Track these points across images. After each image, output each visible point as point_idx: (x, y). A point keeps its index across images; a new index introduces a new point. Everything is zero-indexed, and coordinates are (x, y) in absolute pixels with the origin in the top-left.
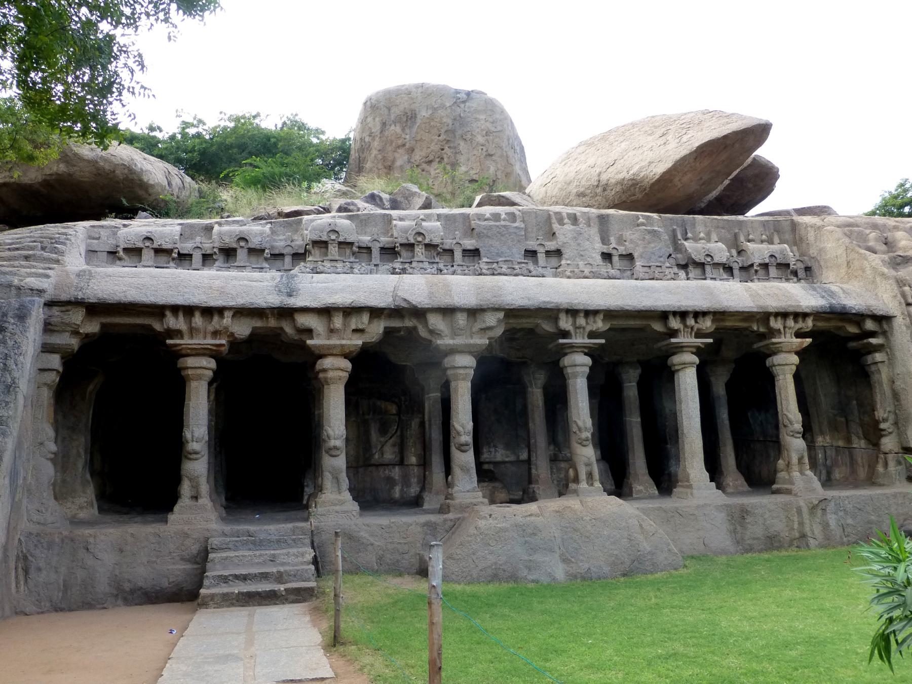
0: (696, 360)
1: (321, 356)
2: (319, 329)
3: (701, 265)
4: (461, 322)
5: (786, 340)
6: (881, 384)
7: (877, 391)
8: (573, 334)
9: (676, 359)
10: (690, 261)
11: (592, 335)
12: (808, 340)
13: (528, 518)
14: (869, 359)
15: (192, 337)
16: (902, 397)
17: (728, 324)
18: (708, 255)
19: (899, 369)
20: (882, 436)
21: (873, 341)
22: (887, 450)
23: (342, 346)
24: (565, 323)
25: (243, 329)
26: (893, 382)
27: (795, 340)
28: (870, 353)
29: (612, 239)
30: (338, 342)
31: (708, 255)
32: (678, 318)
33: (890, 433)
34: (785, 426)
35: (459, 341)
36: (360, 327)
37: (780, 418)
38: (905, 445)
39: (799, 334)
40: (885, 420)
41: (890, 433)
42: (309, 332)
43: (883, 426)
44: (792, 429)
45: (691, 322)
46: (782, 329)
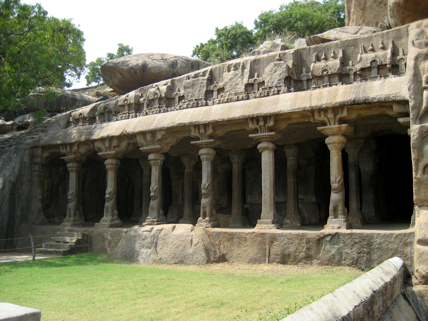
0: (271, 146)
1: (106, 159)
2: (102, 147)
3: (321, 77)
4: (148, 138)
5: (330, 127)
8: (200, 137)
9: (260, 146)
10: (313, 76)
11: (210, 137)
12: (343, 125)
13: (145, 233)
15: (68, 156)
17: (294, 121)
18: (325, 70)
21: (401, 120)
23: (109, 154)
24: (194, 133)
25: (83, 150)
27: (337, 126)
29: (256, 74)
30: (109, 152)
31: (325, 70)
32: (255, 122)
35: (150, 147)
36: (115, 145)
39: (342, 121)
42: (100, 150)
45: (261, 123)
46: (326, 119)
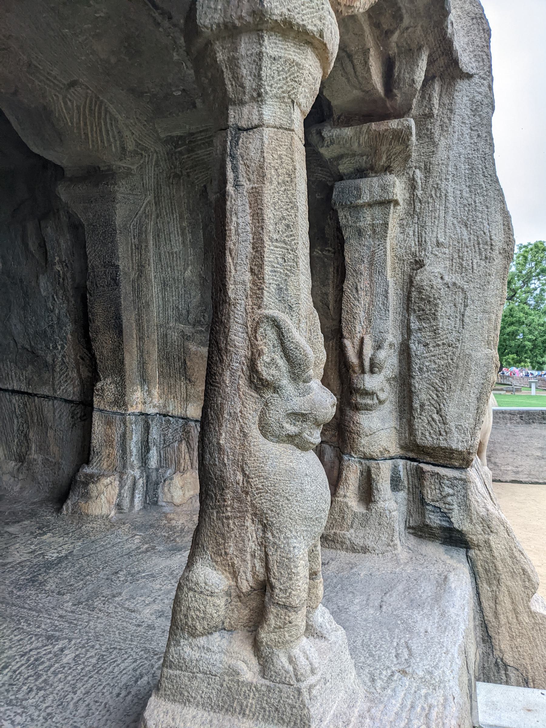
6: (376, 266)
7: (364, 283)
14: (370, 188)
16: (445, 309)
19: (443, 229)
20: (357, 408)
22: (375, 451)
26: (419, 264)
28: (361, 173)
33: (381, 402)
34: (259, 383)
37: (238, 337)
38: (426, 437)
40: (374, 367)
41: (381, 402)
43: (370, 382)
44: (298, 403)
